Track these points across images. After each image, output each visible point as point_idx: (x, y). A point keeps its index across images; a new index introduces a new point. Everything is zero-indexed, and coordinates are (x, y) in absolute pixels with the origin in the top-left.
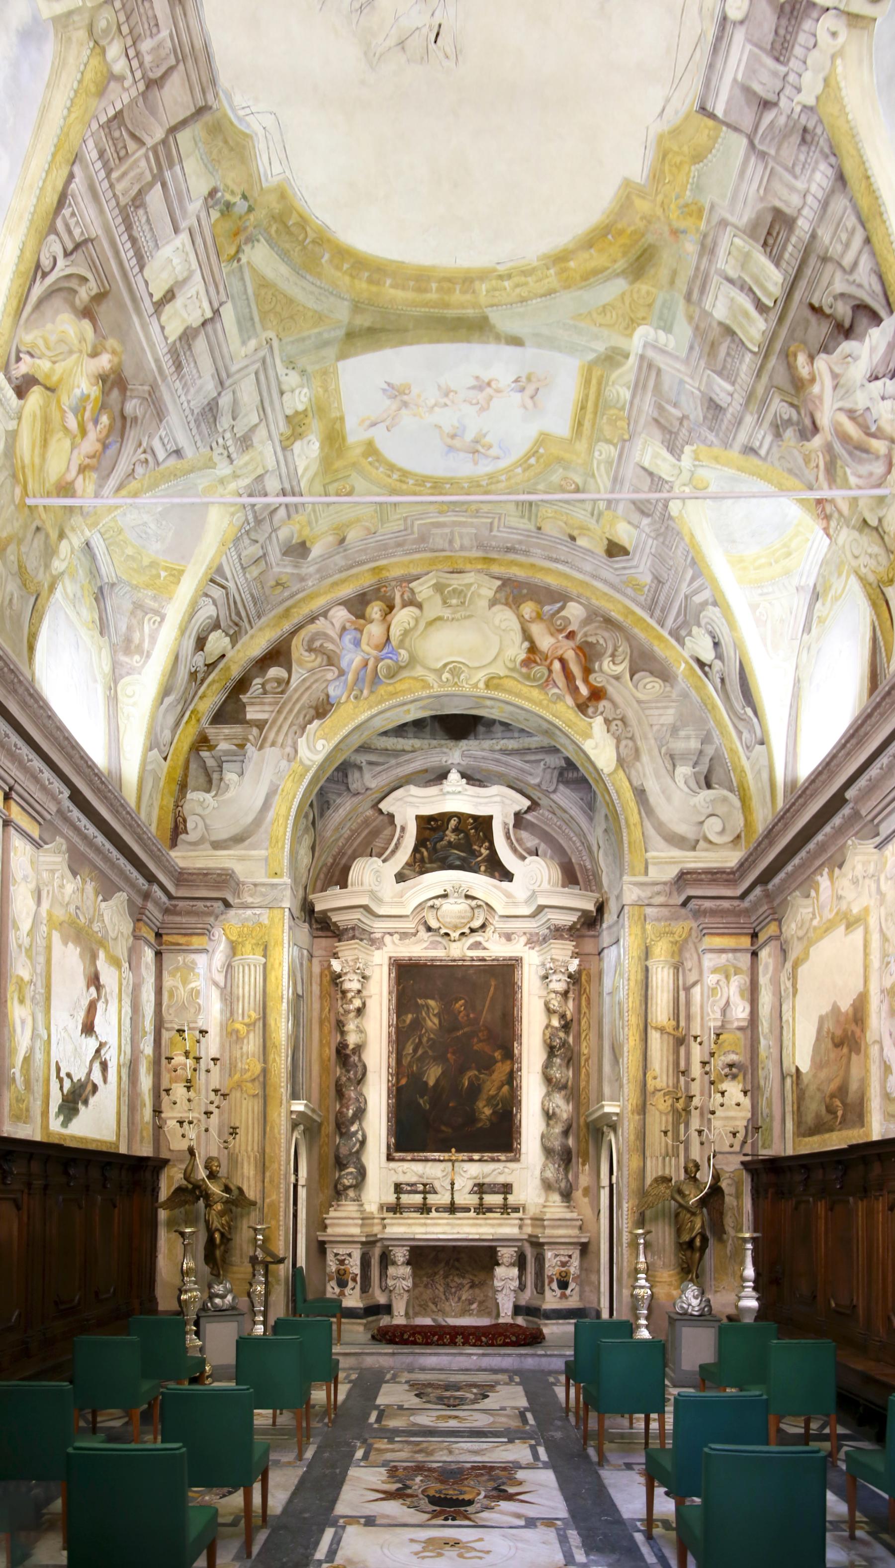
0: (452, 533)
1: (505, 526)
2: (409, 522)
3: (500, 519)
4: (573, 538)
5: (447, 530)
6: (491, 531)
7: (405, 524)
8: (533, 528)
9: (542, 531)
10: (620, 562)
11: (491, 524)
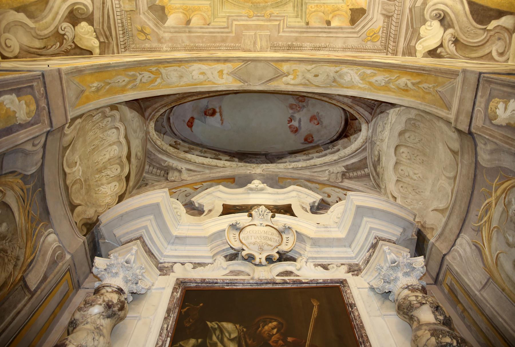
0: (255, 34)
1: (287, 27)
2: (230, 21)
3: (284, 20)
4: (328, 23)
5: (252, 33)
6: (279, 32)
7: (228, 22)
8: (303, 24)
9: (310, 26)
10: (361, 23)
11: (279, 25)
